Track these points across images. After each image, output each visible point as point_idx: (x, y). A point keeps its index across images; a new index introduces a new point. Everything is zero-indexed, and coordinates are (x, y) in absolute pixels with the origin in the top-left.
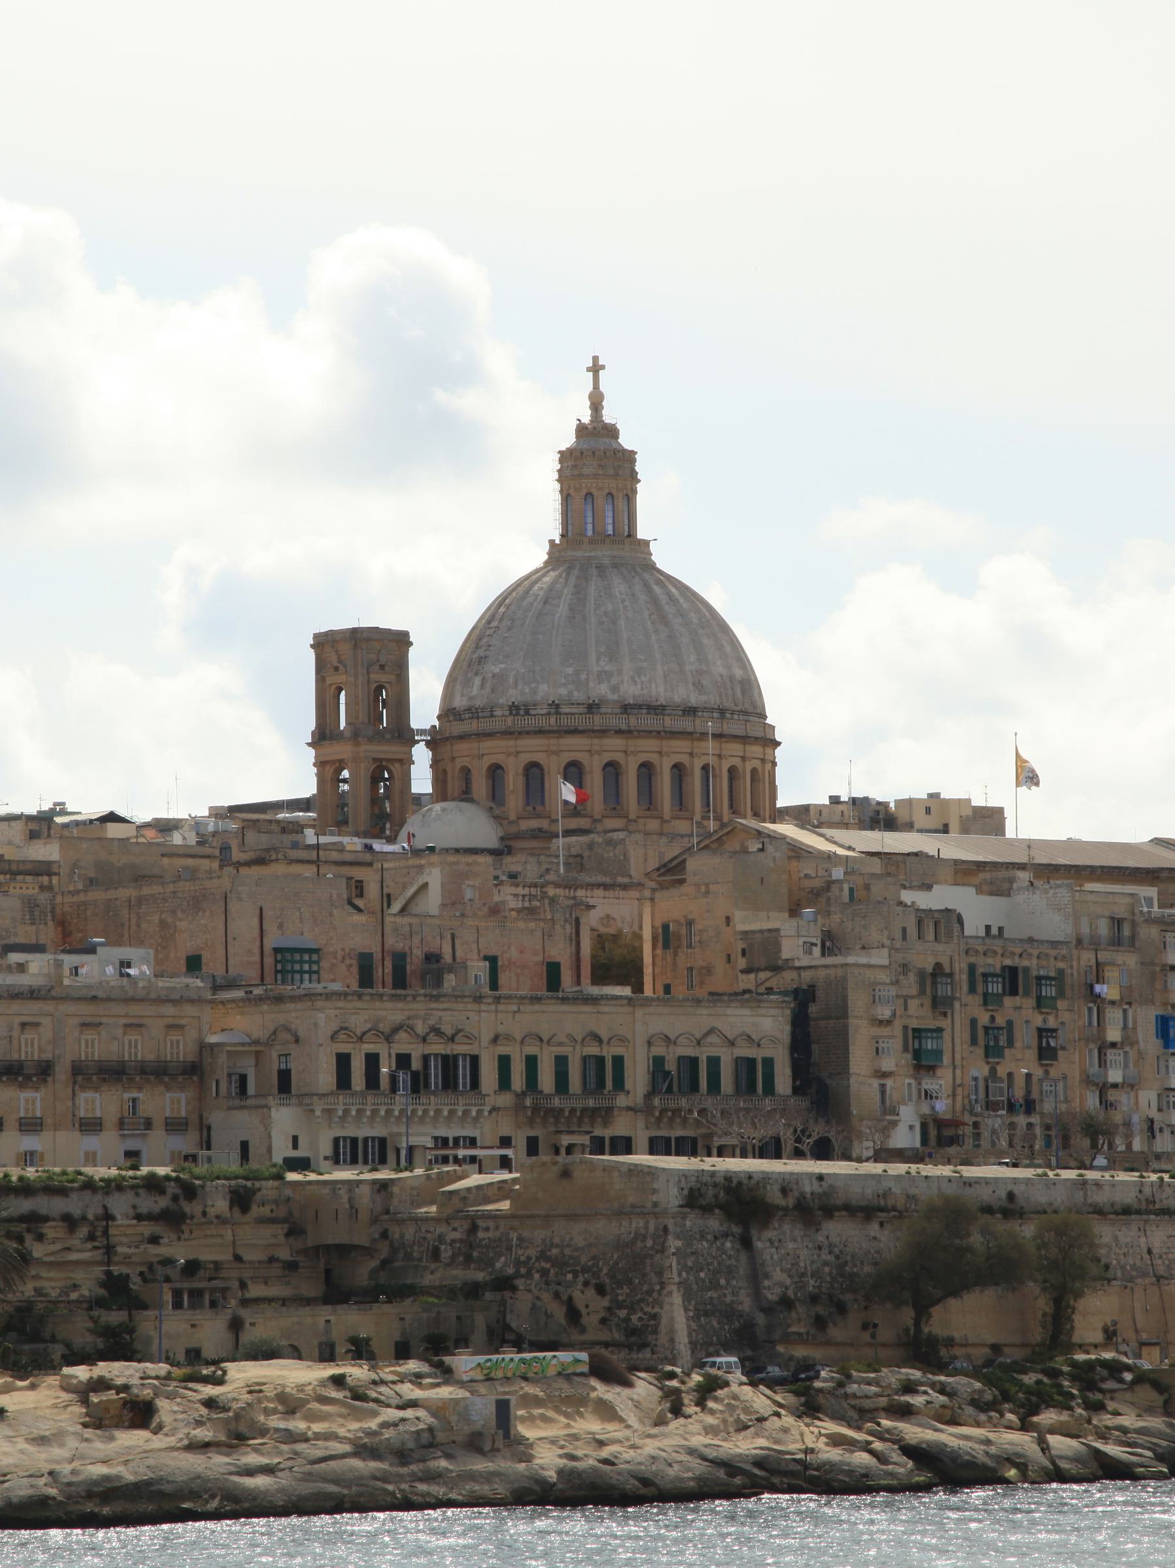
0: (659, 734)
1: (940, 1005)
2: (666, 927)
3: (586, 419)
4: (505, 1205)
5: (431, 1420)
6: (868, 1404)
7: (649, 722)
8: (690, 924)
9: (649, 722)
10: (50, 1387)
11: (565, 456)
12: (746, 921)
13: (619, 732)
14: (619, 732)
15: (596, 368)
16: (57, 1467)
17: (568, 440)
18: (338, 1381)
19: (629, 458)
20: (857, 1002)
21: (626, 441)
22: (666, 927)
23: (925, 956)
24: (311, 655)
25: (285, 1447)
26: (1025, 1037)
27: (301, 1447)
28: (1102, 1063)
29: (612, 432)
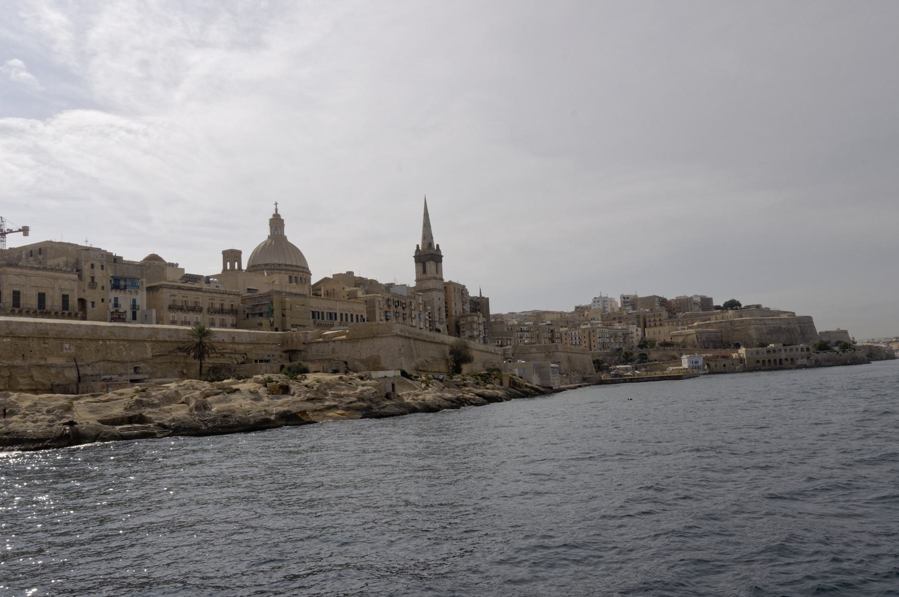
0: (292, 271)
1: (389, 306)
2: (327, 291)
3: (275, 213)
4: (344, 337)
5: (374, 390)
6: (459, 383)
7: (290, 268)
8: (333, 290)
9: (290, 268)
10: (250, 382)
11: (271, 220)
12: (347, 289)
13: (285, 270)
14: (285, 270)
15: (276, 204)
16: (267, 408)
17: (271, 217)
18: (341, 378)
19: (283, 221)
20: (377, 304)
21: (282, 218)
22: (327, 291)
23: (387, 296)
24: (222, 255)
25: (337, 399)
26: (401, 315)
27: (342, 399)
28: (412, 321)
29: (279, 216)
